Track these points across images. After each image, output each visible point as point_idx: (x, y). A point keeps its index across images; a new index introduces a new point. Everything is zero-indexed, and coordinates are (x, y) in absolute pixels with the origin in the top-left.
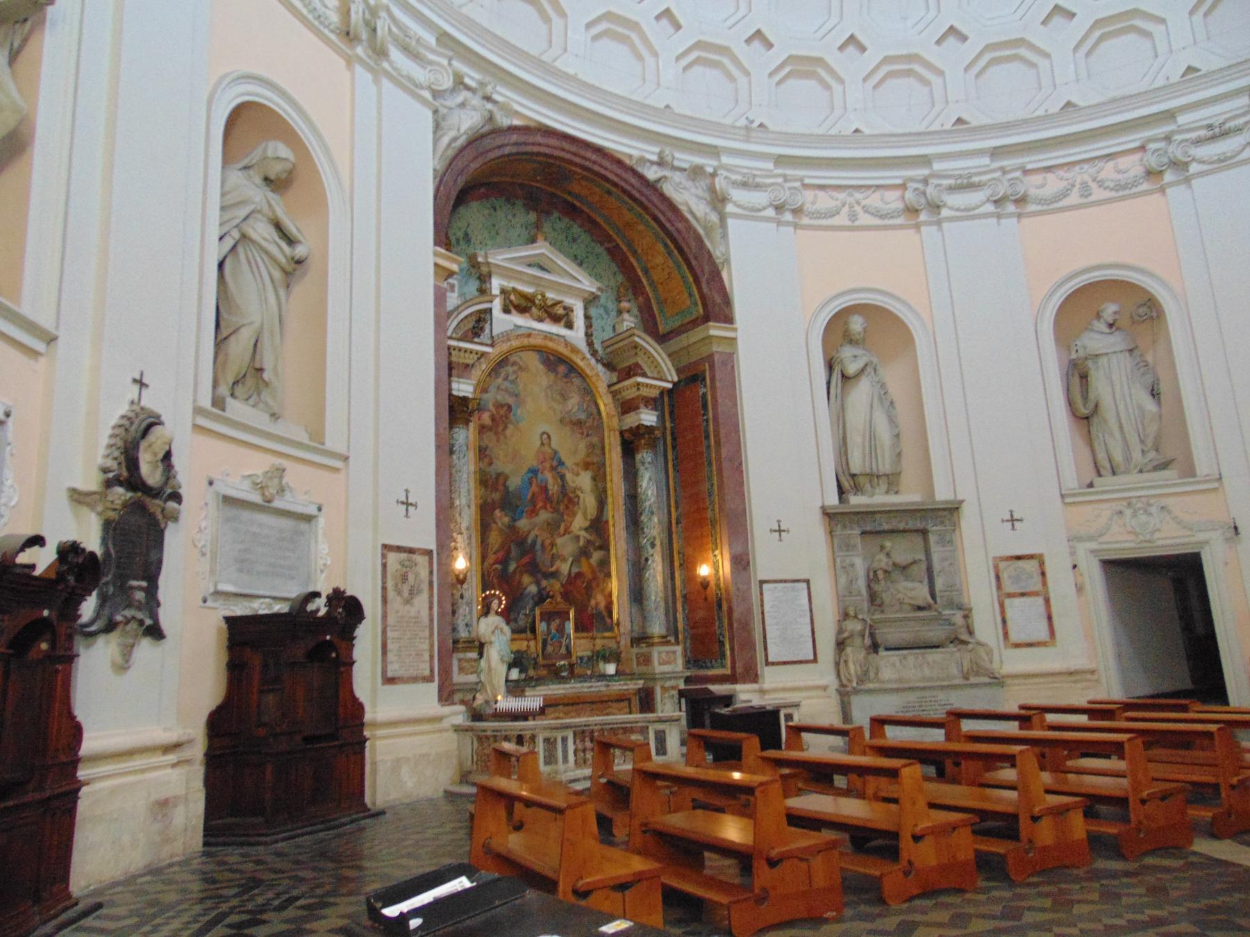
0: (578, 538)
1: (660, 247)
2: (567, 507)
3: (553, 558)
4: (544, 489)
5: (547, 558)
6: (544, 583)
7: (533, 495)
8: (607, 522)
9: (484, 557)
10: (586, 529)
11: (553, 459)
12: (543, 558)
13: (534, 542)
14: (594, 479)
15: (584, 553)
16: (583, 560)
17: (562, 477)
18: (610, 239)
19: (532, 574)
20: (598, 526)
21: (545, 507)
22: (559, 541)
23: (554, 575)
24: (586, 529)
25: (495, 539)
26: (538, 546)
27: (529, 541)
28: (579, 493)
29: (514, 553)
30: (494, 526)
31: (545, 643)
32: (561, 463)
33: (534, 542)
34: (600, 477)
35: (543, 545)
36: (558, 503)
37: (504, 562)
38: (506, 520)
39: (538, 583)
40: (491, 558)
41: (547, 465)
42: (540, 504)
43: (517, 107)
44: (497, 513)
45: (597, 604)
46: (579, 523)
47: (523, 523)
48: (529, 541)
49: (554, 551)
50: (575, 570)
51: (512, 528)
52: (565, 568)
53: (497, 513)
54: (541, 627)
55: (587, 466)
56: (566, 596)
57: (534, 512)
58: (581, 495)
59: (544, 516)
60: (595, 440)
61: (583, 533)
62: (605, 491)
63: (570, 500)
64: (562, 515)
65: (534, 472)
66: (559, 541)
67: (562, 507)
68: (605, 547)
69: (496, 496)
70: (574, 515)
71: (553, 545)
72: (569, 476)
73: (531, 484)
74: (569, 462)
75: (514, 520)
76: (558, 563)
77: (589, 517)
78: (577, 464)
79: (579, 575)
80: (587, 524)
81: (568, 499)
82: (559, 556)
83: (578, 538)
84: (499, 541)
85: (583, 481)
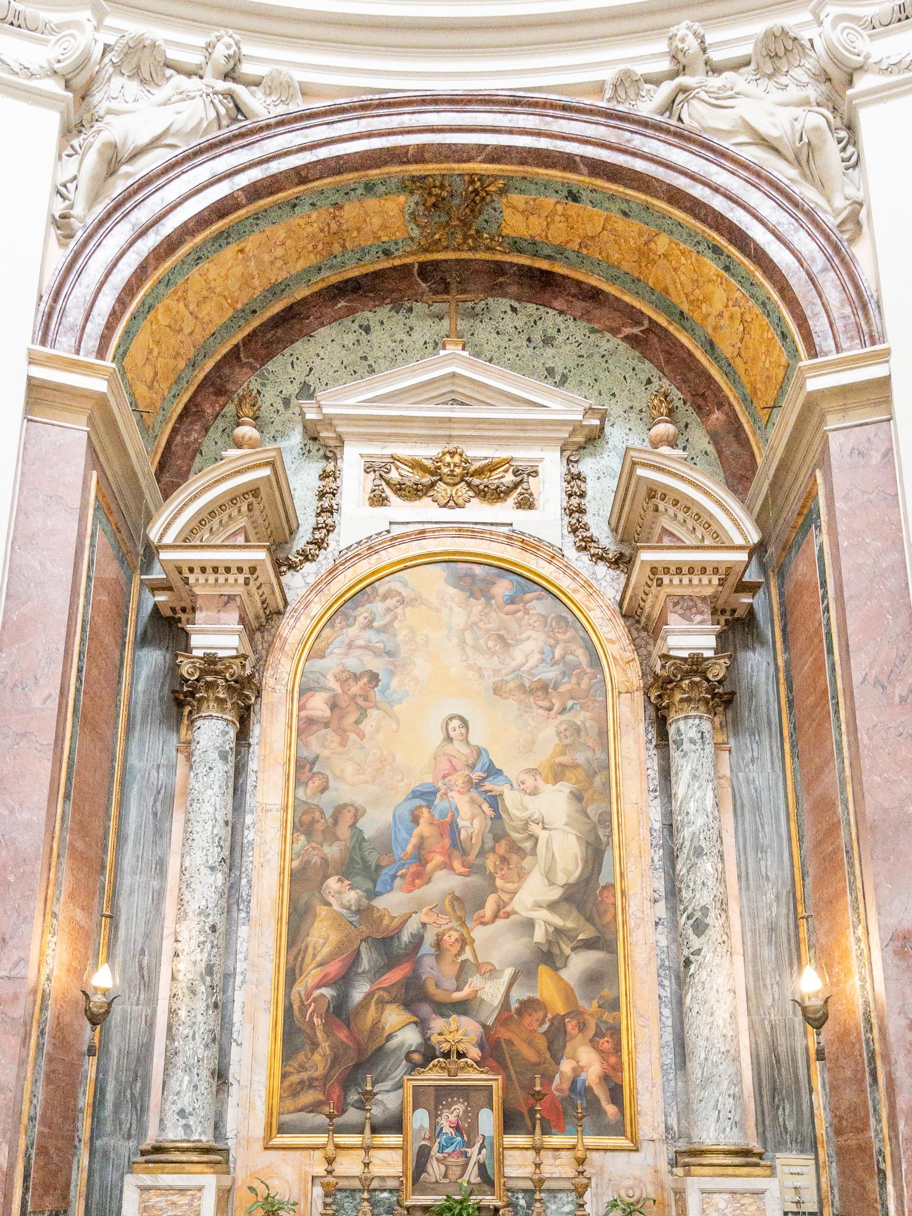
0: (529, 925)
1: (712, 267)
2: (504, 860)
3: (462, 973)
4: (452, 829)
5: (449, 969)
6: (437, 1024)
7: (422, 838)
8: (611, 886)
9: (292, 977)
10: (552, 906)
11: (472, 767)
12: (438, 975)
13: (418, 940)
14: (577, 797)
15: (548, 956)
16: (543, 970)
17: (495, 801)
18: (634, 316)
19: (408, 1005)
20: (588, 897)
21: (447, 866)
22: (479, 933)
23: (463, 1008)
24: (552, 906)
25: (323, 936)
26: (427, 947)
27: (405, 938)
28: (536, 829)
29: (365, 964)
30: (322, 910)
31: (423, 1155)
32: (492, 771)
33: (418, 940)
34: (592, 787)
35: (438, 945)
36: (482, 853)
37: (344, 981)
38: (352, 896)
39: (422, 1025)
40: (311, 975)
41: (458, 780)
42: (438, 859)
43: (299, 76)
44: (333, 883)
45: (578, 1070)
46: (533, 895)
47: (392, 902)
48: (405, 938)
49: (467, 955)
50: (519, 994)
51: (364, 912)
52: (492, 992)
53: (333, 883)
54: (419, 1119)
55: (558, 773)
56: (492, 1051)
57: (420, 876)
58: (543, 835)
59: (445, 881)
60: (580, 717)
61: (543, 915)
62: (605, 820)
63: (515, 848)
64: (492, 878)
65: (427, 795)
66: (479, 933)
67: (491, 862)
68: (603, 941)
69: (332, 851)
70: (522, 875)
71: (464, 942)
72: (511, 799)
73: (416, 820)
74: (512, 767)
75: (372, 894)
76: (475, 982)
77: (562, 879)
78: (533, 771)
79: (528, 1006)
80: (556, 894)
81: (507, 844)
82: (478, 966)
83: (529, 925)
84: (334, 937)
85: (554, 804)
